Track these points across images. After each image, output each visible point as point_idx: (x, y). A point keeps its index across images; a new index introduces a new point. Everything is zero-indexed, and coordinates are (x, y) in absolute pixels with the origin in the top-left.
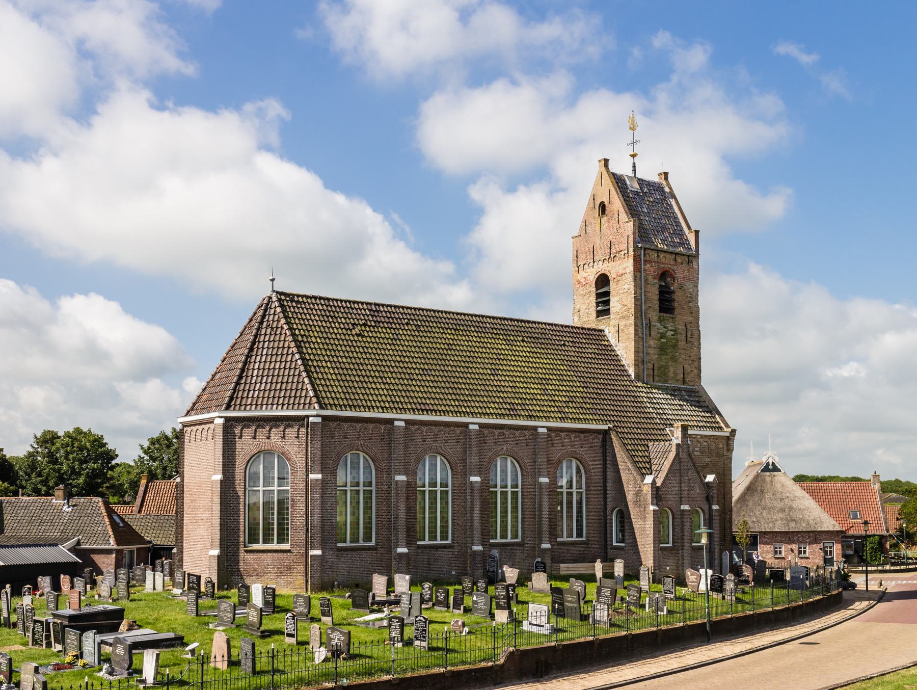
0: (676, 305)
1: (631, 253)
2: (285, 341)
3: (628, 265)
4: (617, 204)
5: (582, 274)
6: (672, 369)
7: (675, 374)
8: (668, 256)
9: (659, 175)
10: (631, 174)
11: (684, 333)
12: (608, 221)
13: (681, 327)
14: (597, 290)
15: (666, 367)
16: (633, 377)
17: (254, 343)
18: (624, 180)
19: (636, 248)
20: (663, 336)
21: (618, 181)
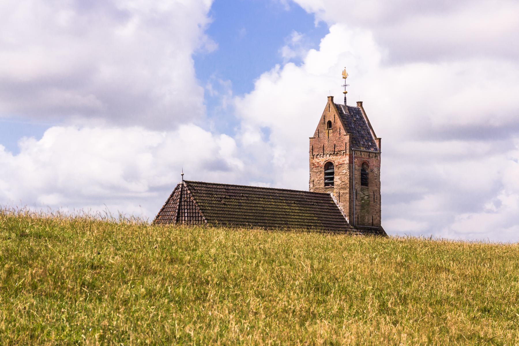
0: (369, 181)
1: (348, 153)
2: (195, 209)
3: (346, 159)
4: (339, 123)
5: (316, 160)
6: (367, 217)
7: (369, 220)
8: (366, 154)
9: (358, 103)
10: (343, 104)
11: (373, 197)
12: (333, 132)
13: (372, 194)
14: (325, 170)
15: (364, 216)
16: (348, 222)
17: (179, 210)
18: (341, 108)
19: (350, 149)
20: (363, 199)
21: (338, 107)
